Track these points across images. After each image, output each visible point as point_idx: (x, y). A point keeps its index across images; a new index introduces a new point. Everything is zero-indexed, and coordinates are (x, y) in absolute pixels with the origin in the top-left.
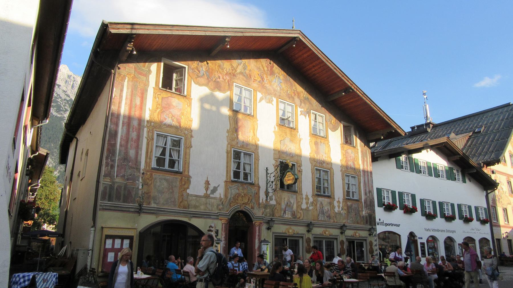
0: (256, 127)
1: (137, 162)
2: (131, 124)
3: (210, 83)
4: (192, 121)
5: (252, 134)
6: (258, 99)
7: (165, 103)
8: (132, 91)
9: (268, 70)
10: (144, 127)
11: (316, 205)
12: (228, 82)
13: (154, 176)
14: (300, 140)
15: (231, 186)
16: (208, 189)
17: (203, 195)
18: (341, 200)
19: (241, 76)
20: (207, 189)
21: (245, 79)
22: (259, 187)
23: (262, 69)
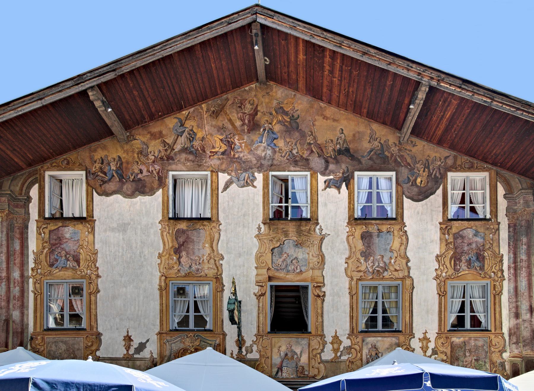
0: (216, 235)
1: (24, 326)
2: (11, 277)
3: (125, 187)
4: (96, 254)
5: (208, 250)
6: (221, 186)
7: (55, 237)
8: (7, 234)
9: (243, 124)
10: (28, 278)
11: (361, 350)
12: (158, 173)
13: (47, 340)
14: (322, 239)
15: (169, 338)
16: (129, 348)
17: (121, 357)
18: (432, 335)
19: (184, 156)
20: (128, 348)
21: (191, 157)
22: (224, 335)
23: (230, 127)
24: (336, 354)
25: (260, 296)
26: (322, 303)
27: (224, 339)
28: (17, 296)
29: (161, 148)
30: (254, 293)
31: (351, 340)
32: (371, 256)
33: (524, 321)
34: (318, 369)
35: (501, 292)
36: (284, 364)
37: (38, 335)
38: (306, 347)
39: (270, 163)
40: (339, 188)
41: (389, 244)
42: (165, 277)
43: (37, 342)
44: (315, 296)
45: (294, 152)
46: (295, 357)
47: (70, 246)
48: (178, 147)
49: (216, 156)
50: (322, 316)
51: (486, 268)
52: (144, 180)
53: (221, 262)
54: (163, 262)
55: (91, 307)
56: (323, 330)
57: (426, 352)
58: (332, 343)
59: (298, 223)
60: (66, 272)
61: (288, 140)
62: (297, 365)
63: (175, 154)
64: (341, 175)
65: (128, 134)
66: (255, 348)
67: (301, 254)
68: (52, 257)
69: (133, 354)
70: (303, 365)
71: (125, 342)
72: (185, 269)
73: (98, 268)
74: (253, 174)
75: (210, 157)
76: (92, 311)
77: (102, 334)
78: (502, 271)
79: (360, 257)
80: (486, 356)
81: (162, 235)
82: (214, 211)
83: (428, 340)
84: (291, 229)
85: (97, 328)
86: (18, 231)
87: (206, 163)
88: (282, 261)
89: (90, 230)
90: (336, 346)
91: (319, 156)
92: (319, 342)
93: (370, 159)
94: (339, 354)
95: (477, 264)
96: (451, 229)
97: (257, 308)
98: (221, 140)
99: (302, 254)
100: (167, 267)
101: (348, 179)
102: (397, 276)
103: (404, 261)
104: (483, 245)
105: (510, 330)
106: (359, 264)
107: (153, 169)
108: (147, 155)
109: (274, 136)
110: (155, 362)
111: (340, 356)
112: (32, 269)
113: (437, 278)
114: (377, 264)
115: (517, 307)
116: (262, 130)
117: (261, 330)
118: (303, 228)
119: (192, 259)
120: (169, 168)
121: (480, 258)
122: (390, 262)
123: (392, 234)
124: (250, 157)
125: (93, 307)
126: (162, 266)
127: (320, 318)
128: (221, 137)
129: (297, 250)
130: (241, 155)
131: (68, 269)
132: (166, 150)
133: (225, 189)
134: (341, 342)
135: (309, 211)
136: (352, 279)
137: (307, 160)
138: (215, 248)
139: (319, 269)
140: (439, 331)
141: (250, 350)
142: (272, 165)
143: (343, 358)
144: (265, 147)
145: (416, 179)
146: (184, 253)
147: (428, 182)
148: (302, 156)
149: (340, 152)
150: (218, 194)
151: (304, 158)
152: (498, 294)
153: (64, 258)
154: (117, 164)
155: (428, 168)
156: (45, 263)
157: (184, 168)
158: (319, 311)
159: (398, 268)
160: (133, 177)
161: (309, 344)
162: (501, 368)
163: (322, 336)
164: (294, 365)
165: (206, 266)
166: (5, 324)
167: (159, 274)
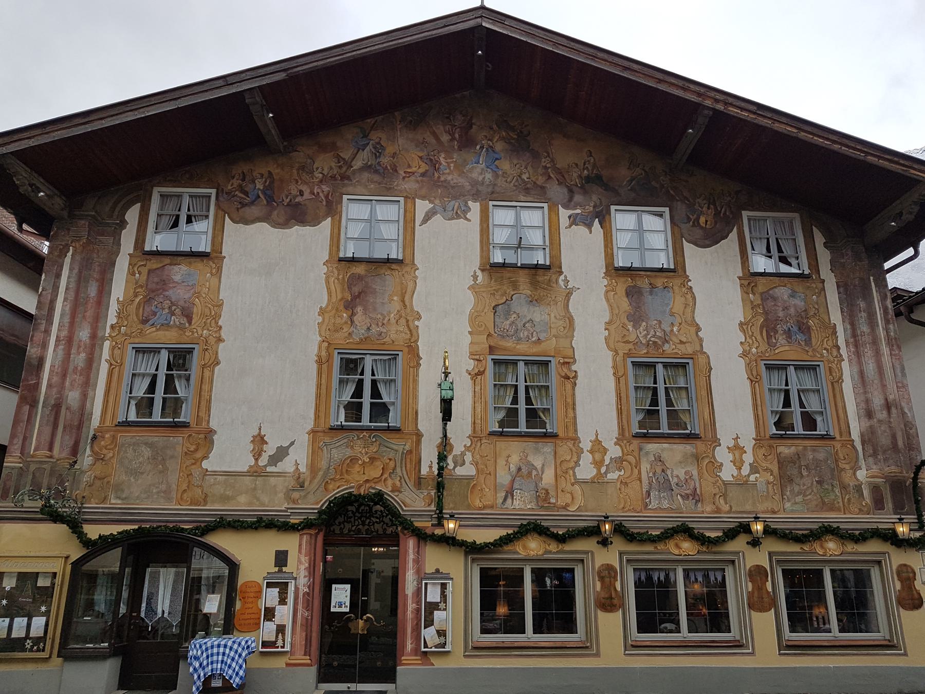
0: (410, 285)
1: (83, 415)
2: (75, 338)
3: (275, 213)
4: (220, 306)
5: (396, 305)
6: (419, 217)
7: (156, 280)
8: (80, 272)
9: (453, 139)
10: (104, 339)
11: (638, 464)
12: (327, 197)
13: (119, 440)
14: (569, 294)
15: (327, 439)
16: (260, 455)
17: (245, 470)
18: (748, 442)
19: (366, 175)
20: (257, 455)
21: (376, 178)
22: (419, 435)
23: (434, 141)
24: (599, 470)
25: (477, 374)
26: (574, 389)
27: (418, 442)
28: (79, 368)
29: (333, 165)
30: (467, 370)
31: (621, 446)
32: (643, 321)
33: (879, 421)
34: (572, 494)
35: (840, 380)
36: (516, 486)
37: (107, 431)
38: (551, 458)
39: (490, 189)
40: (589, 226)
41: (668, 304)
42: (328, 344)
43: (103, 443)
44: (562, 377)
45: (525, 177)
46: (534, 473)
47: (179, 294)
48: (357, 164)
49: (413, 178)
50: (574, 409)
51: (814, 344)
52: (305, 205)
53: (416, 323)
54: (327, 321)
55: (203, 387)
56: (576, 431)
57: (740, 469)
58: (591, 452)
59: (533, 271)
60: (167, 333)
61: (515, 162)
62: (536, 486)
63: (354, 172)
64: (592, 209)
65: (285, 143)
66: (468, 457)
67: (538, 314)
68: (148, 309)
69: (265, 466)
70: (546, 487)
71: (254, 445)
72: (360, 331)
73: (221, 327)
74: (466, 203)
75: (404, 178)
76: (203, 393)
77: (215, 432)
78: (838, 348)
79: (627, 322)
80: (833, 475)
81: (327, 282)
82: (408, 251)
83: (742, 450)
84: (521, 279)
85: (208, 422)
86: (97, 269)
87: (397, 185)
88: (510, 325)
89: (214, 271)
90: (598, 456)
91: (560, 184)
92: (571, 450)
93: (631, 190)
94: (603, 470)
95: (800, 337)
96: (756, 286)
97: (471, 394)
98: (421, 158)
99: (539, 315)
100: (332, 328)
101: (603, 216)
102: (684, 351)
103: (693, 330)
104: (805, 310)
105: (862, 435)
106: (625, 332)
107: (319, 191)
108: (311, 172)
109: (496, 156)
110: (301, 480)
111: (606, 473)
112: (112, 327)
113: (744, 355)
114: (652, 333)
115: (867, 401)
116: (478, 147)
117: (478, 428)
118: (540, 279)
119: (371, 318)
120: (344, 190)
121: (804, 329)
122: (672, 330)
123: (671, 290)
124: (462, 181)
125: (206, 387)
126: (324, 327)
127: (570, 411)
128: (421, 154)
129: (532, 309)
130: (449, 178)
131: (171, 327)
132: (340, 167)
133: (425, 221)
134: (605, 451)
135: (548, 256)
136: (616, 352)
137: (543, 188)
138: (407, 303)
139: (567, 337)
140: (757, 436)
141: (460, 461)
142: (493, 193)
143: (610, 476)
144: (483, 169)
145: (698, 219)
146: (359, 309)
147: (716, 223)
148: (535, 183)
149: (588, 179)
150: (414, 228)
151: (538, 186)
152: (838, 382)
153: (167, 311)
154: (266, 182)
155: (715, 205)
156: (135, 318)
157: (365, 191)
158: (569, 400)
159: (684, 340)
160: (288, 200)
161: (555, 453)
162: (856, 495)
163: (576, 440)
164: (532, 487)
165: (393, 328)
166: (54, 413)
167: (319, 339)
